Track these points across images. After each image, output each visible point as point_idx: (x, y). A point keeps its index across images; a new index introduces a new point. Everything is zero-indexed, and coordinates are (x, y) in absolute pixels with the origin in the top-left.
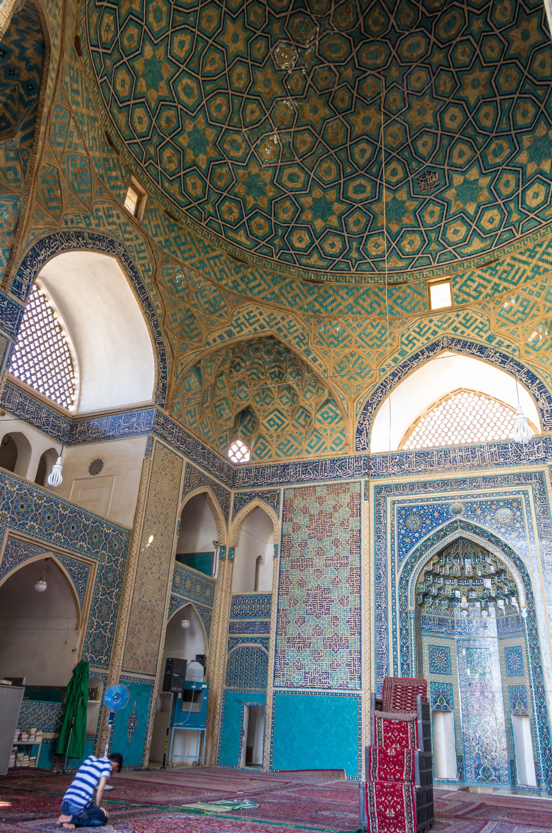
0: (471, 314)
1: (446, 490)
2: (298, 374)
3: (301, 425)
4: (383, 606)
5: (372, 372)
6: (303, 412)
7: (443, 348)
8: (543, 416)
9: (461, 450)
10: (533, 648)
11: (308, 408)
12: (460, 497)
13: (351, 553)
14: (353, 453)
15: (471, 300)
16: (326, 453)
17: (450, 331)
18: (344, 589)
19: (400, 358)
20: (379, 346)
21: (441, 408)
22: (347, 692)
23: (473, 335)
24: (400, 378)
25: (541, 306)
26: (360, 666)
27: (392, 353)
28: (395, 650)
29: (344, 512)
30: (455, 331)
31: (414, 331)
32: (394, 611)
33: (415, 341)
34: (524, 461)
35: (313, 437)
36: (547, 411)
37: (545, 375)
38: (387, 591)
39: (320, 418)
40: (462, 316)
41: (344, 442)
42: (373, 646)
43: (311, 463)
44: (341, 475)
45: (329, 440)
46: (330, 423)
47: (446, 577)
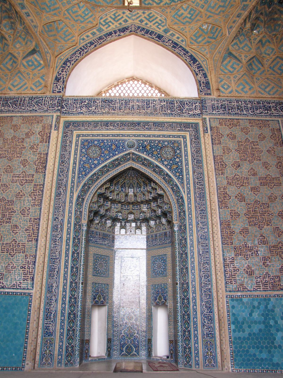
0: (153, 13)
1: (123, 129)
2: (12, 28)
3: (8, 69)
4: (60, 218)
5: (74, 38)
6: (11, 59)
7: (131, 31)
8: (200, 85)
9: (138, 101)
10: (182, 254)
11: (16, 55)
12: (134, 136)
13: (37, 171)
14: (48, 94)
15: (155, 4)
16: (26, 91)
17: (137, 21)
18: (27, 202)
19: (98, 33)
20: (82, 22)
21: (117, 88)
22: (19, 291)
23: (154, 27)
24: (95, 46)
25: (203, 14)
26: (34, 268)
27: (92, 28)
28: (67, 255)
29: (35, 139)
30: (141, 22)
31: (111, 17)
32: (69, 222)
33: (110, 24)
34: (185, 114)
35: (17, 78)
36: (203, 82)
37: (202, 59)
38: (65, 206)
39: (25, 64)
40: (147, 14)
41: (43, 85)
42: (47, 251)
43: (11, 98)
44: (37, 109)
45: (30, 82)
46: (33, 70)
47: (113, 201)
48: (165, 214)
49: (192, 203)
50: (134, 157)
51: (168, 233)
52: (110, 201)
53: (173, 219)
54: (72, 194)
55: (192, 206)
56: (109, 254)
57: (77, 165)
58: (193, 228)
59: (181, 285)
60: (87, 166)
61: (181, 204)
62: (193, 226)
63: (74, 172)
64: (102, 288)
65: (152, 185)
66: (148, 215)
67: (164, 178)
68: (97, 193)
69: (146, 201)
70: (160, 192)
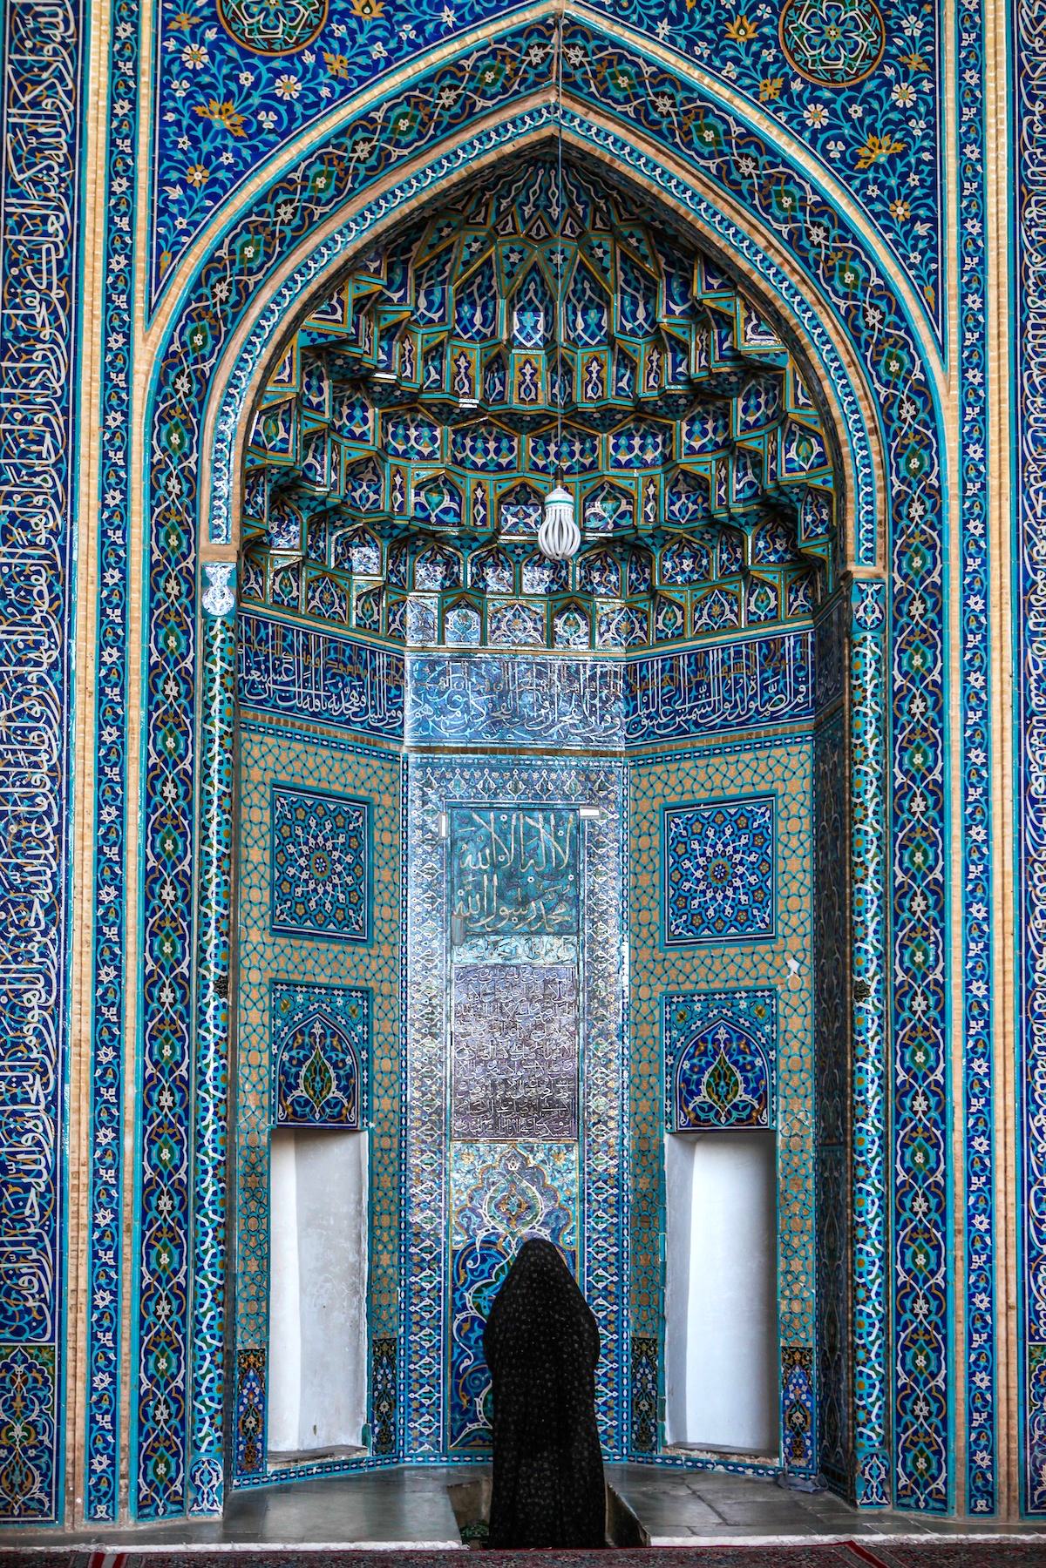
4: (42, 525)
10: (902, 793)
38: (71, 429)
47: (402, 406)
48: (776, 512)
49: (992, 436)
50: (576, 56)
51: (790, 642)
52: (375, 403)
53: (851, 549)
54: (116, 341)
55: (993, 457)
56: (374, 783)
57: (145, 103)
58: (994, 613)
59: (892, 1004)
60: (219, 122)
61: (910, 439)
62: (994, 598)
63: (120, 166)
64: (335, 1013)
65: (697, 289)
66: (646, 516)
67: (794, 240)
68: (300, 339)
69: (640, 405)
70: (758, 343)
